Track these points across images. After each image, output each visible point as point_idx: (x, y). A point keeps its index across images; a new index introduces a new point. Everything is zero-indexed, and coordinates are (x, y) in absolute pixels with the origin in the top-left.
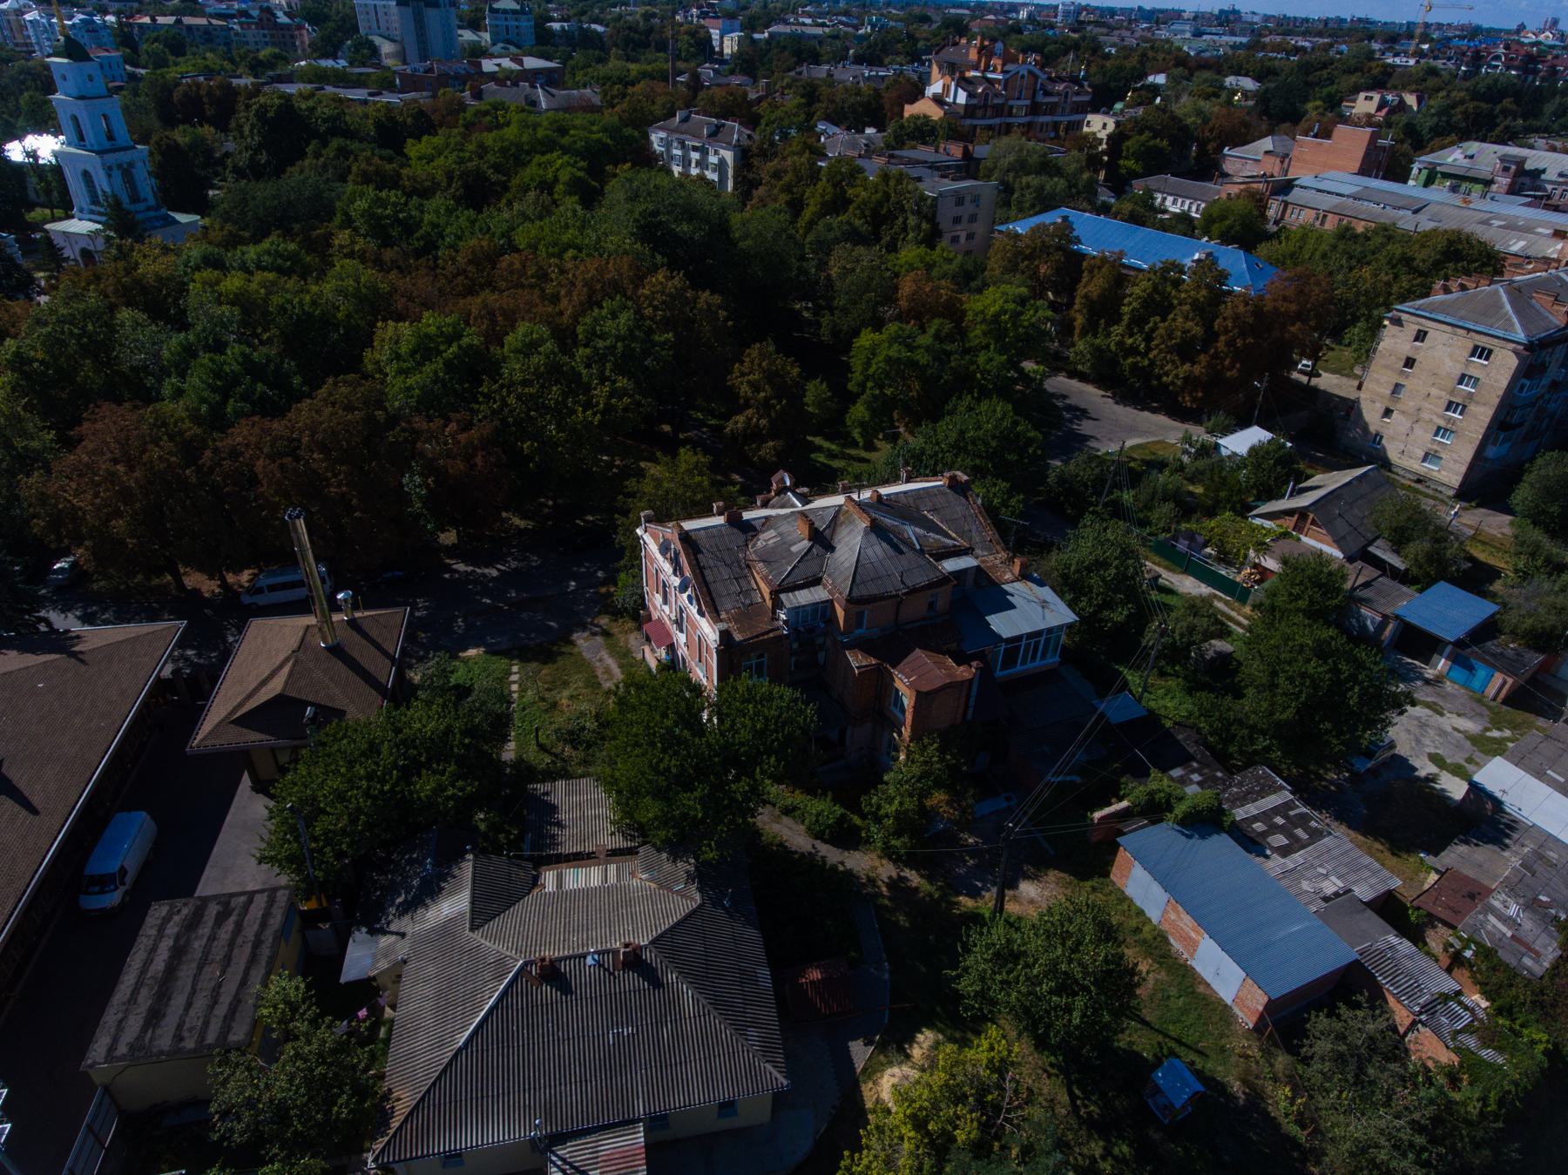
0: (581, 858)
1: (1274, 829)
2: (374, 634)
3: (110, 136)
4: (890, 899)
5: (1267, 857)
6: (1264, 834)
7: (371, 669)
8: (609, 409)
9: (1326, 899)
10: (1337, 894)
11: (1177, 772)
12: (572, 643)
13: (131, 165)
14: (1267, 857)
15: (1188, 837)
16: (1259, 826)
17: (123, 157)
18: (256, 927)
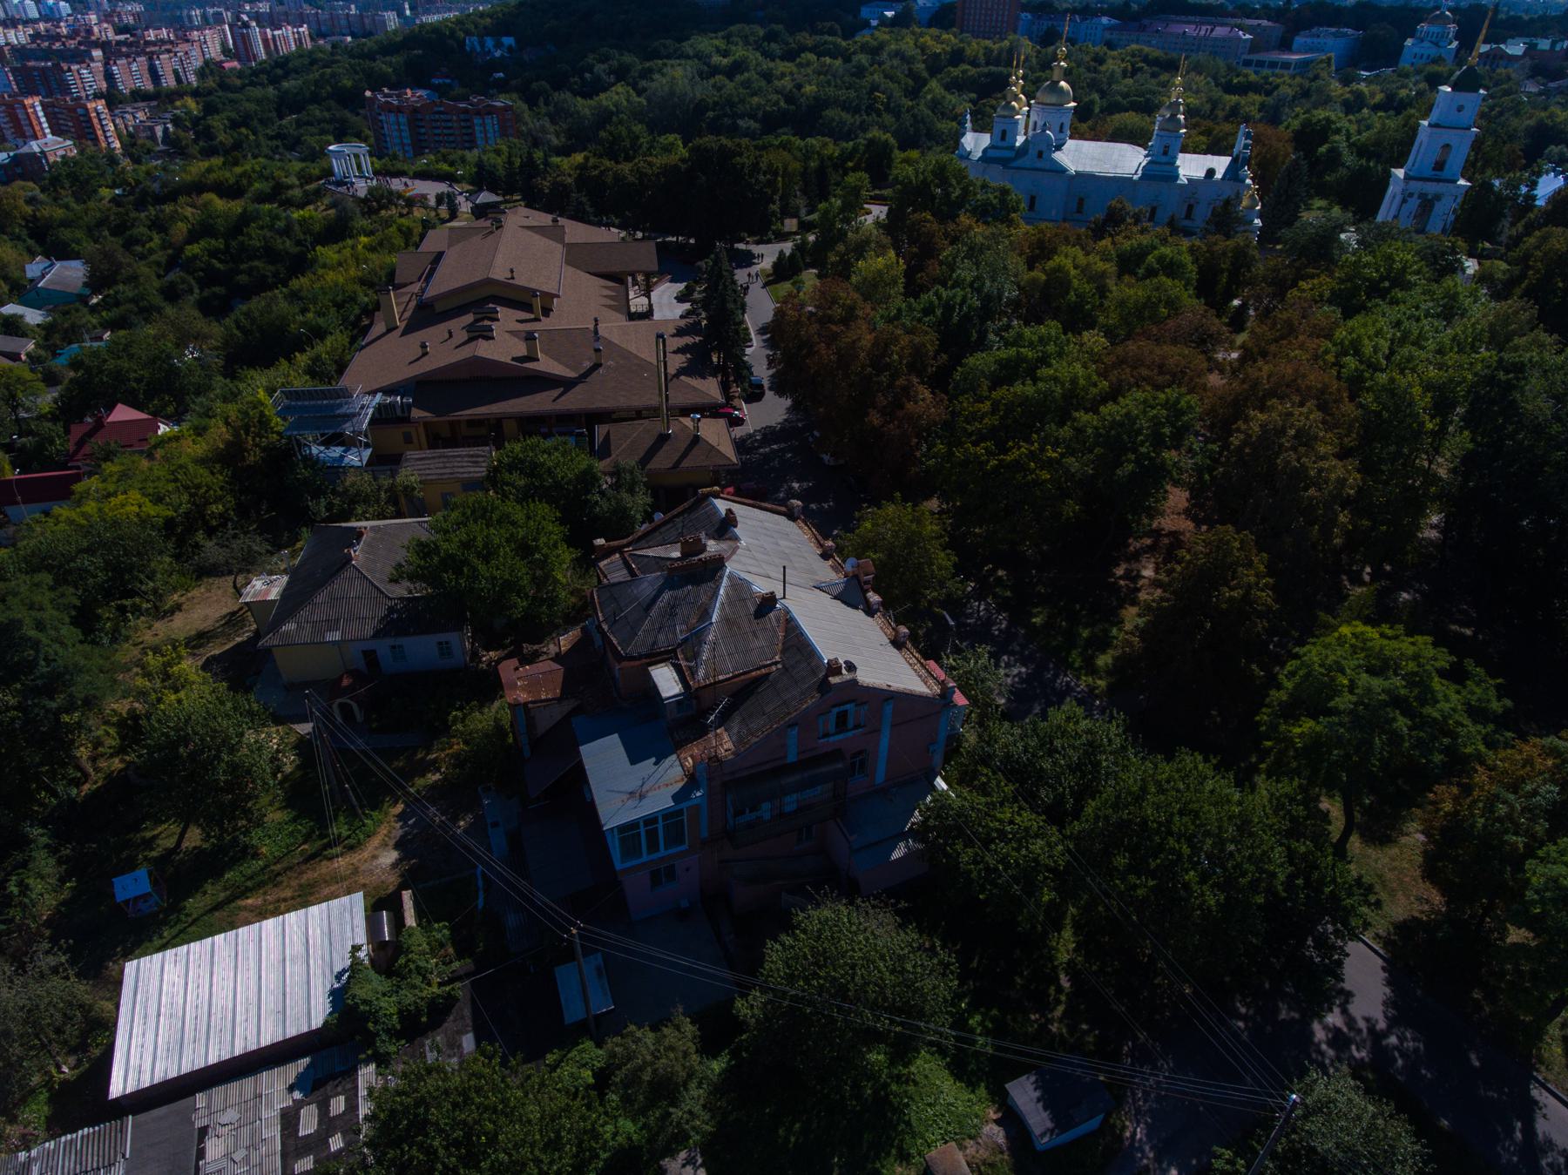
1: (328, 1125)
2: (695, 451)
3: (1439, 166)
4: (423, 759)
5: (291, 1089)
6: (324, 1107)
8: (1017, 465)
9: (203, 1131)
10: (201, 1154)
11: (468, 1042)
13: (1438, 197)
14: (291, 1089)
15: (339, 977)
16: (338, 1105)
17: (1431, 188)
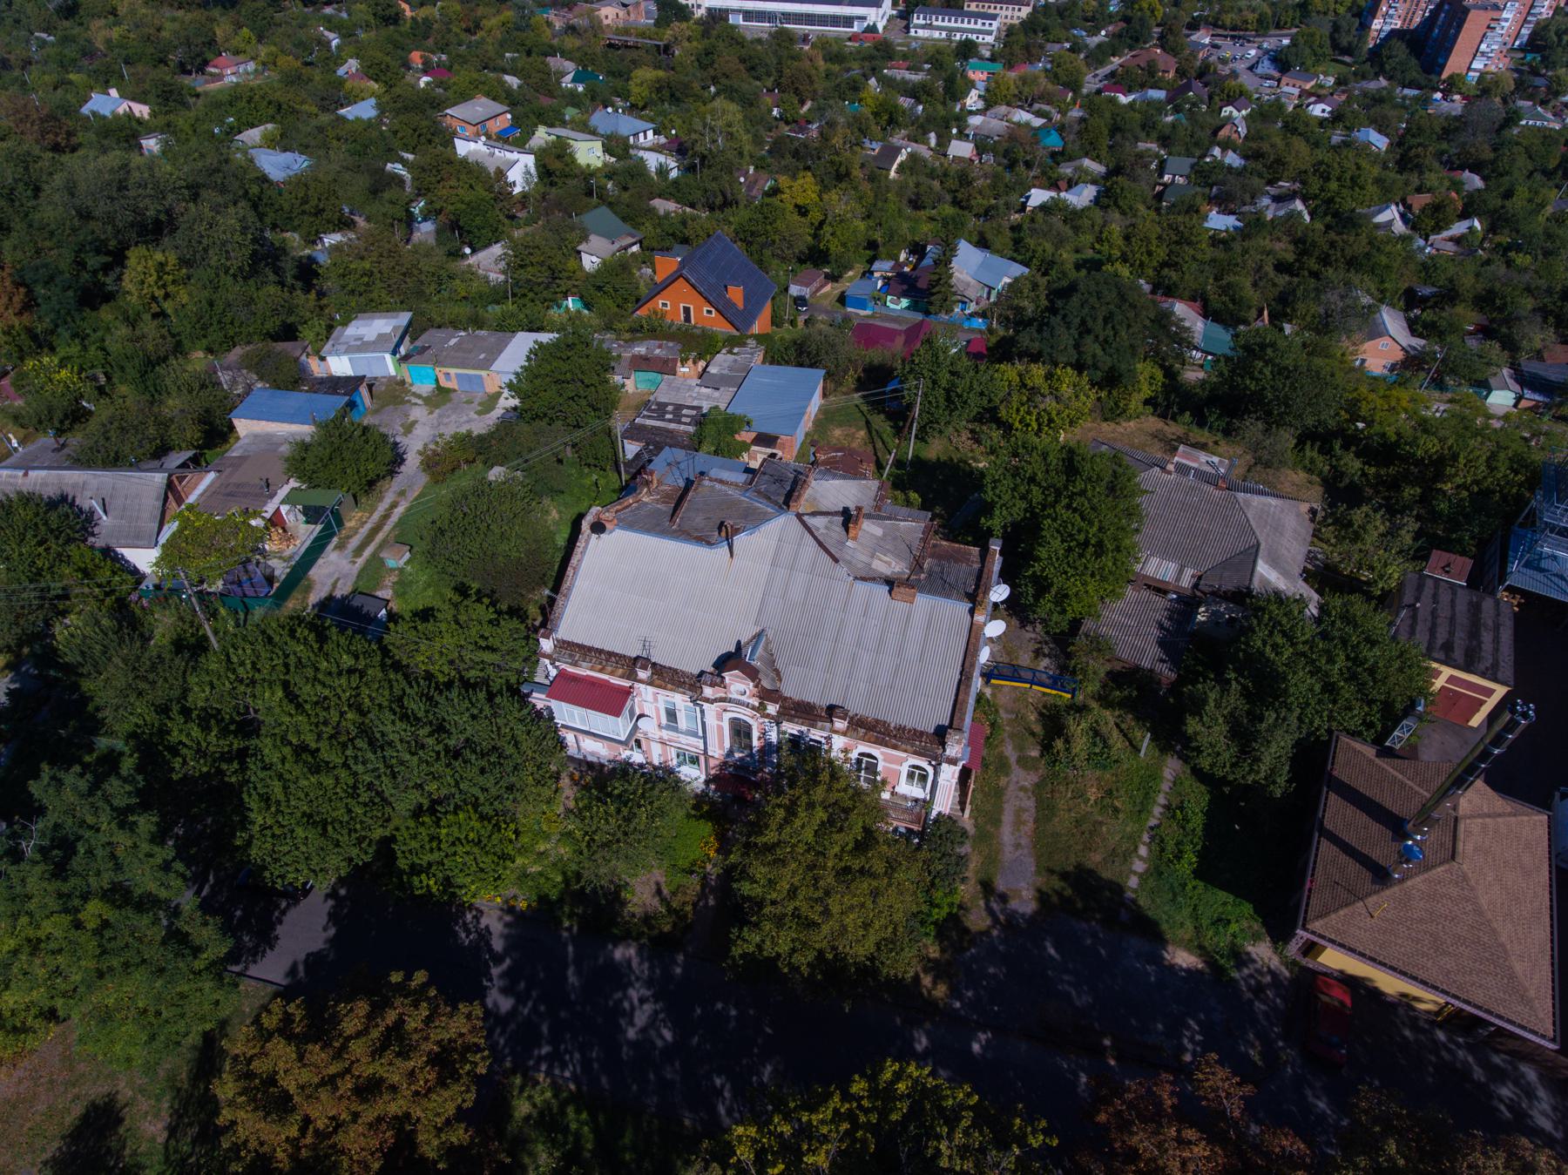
0: (1159, 589)
2: (1353, 867)
7: (1350, 811)
12: (1042, 897)
18: (1418, 628)
